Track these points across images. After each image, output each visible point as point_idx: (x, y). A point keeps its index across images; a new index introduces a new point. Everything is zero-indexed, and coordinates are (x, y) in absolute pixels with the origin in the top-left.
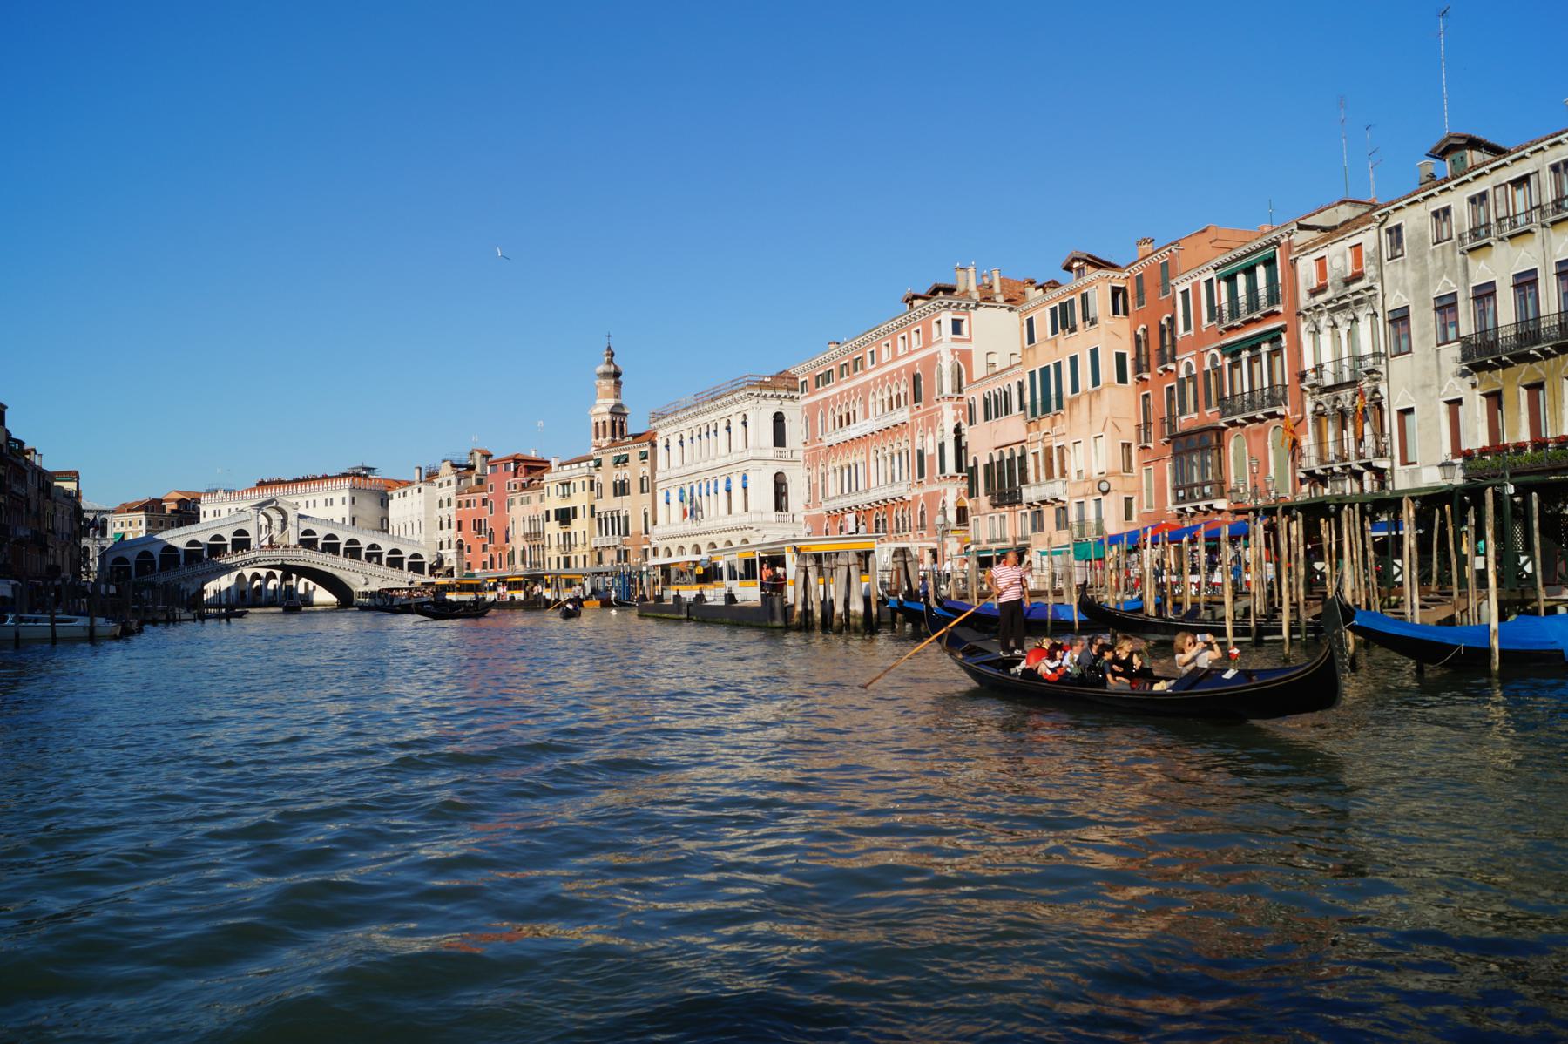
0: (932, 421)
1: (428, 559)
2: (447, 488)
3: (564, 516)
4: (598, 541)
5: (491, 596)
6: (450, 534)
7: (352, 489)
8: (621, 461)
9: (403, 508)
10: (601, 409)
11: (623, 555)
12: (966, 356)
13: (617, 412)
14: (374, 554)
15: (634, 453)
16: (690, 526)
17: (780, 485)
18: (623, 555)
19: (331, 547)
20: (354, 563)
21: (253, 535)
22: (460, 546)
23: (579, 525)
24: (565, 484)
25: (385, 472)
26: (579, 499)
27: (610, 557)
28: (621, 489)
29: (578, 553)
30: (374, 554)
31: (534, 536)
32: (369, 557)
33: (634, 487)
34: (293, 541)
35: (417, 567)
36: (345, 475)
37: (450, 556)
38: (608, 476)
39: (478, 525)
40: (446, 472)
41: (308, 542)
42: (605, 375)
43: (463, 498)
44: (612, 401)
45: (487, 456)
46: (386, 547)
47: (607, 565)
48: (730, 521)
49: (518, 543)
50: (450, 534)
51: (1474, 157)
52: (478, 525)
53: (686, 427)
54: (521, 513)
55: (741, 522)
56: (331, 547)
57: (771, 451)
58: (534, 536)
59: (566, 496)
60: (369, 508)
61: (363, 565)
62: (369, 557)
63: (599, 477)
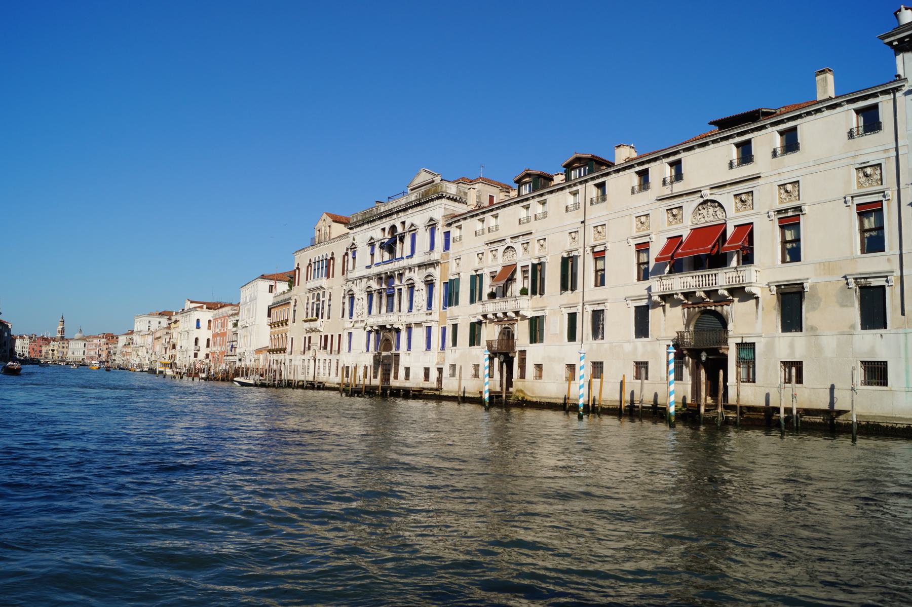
3: (53, 351)
26: (56, 348)
31: (47, 353)
38: (61, 345)
58: (47, 353)
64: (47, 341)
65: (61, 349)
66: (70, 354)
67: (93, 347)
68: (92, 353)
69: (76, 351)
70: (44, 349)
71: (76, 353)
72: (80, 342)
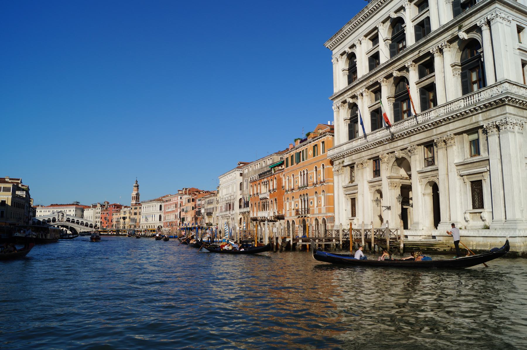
0: (177, 211)
1: (94, 225)
2: (99, 209)
3: (124, 218)
4: (130, 224)
5: (110, 233)
6: (99, 220)
8: (136, 208)
9: (87, 213)
10: (134, 194)
12: (182, 202)
13: (138, 194)
14: (82, 224)
15: (138, 207)
16: (146, 222)
17: (160, 217)
18: (135, 226)
19: (73, 222)
20: (78, 225)
22: (101, 222)
23: (127, 220)
24: (125, 212)
25: (82, 203)
26: (127, 215)
27: (133, 227)
28: (135, 214)
29: (126, 226)
30: (82, 224)
31: (118, 222)
32: (81, 224)
34: (65, 220)
35: (91, 226)
36: (73, 204)
37: (99, 224)
38: (133, 211)
39: (105, 218)
40: (99, 206)
41: (68, 220)
42: (135, 186)
43: (103, 212)
44: (136, 192)
45: (108, 203)
46: (85, 222)
47: (132, 228)
48: (152, 222)
49: (114, 223)
50: (99, 220)
51: (213, 195)
52: (105, 218)
54: (115, 217)
55: (154, 222)
56: (73, 222)
57: (159, 211)
58: (118, 222)
60: (79, 212)
61: (80, 226)
62: (81, 224)
63: (131, 211)
65: (133, 216)
66: (143, 221)
67: (172, 208)
68: (171, 218)
69: (150, 217)
70: (115, 217)
71: (150, 219)
72: (154, 203)
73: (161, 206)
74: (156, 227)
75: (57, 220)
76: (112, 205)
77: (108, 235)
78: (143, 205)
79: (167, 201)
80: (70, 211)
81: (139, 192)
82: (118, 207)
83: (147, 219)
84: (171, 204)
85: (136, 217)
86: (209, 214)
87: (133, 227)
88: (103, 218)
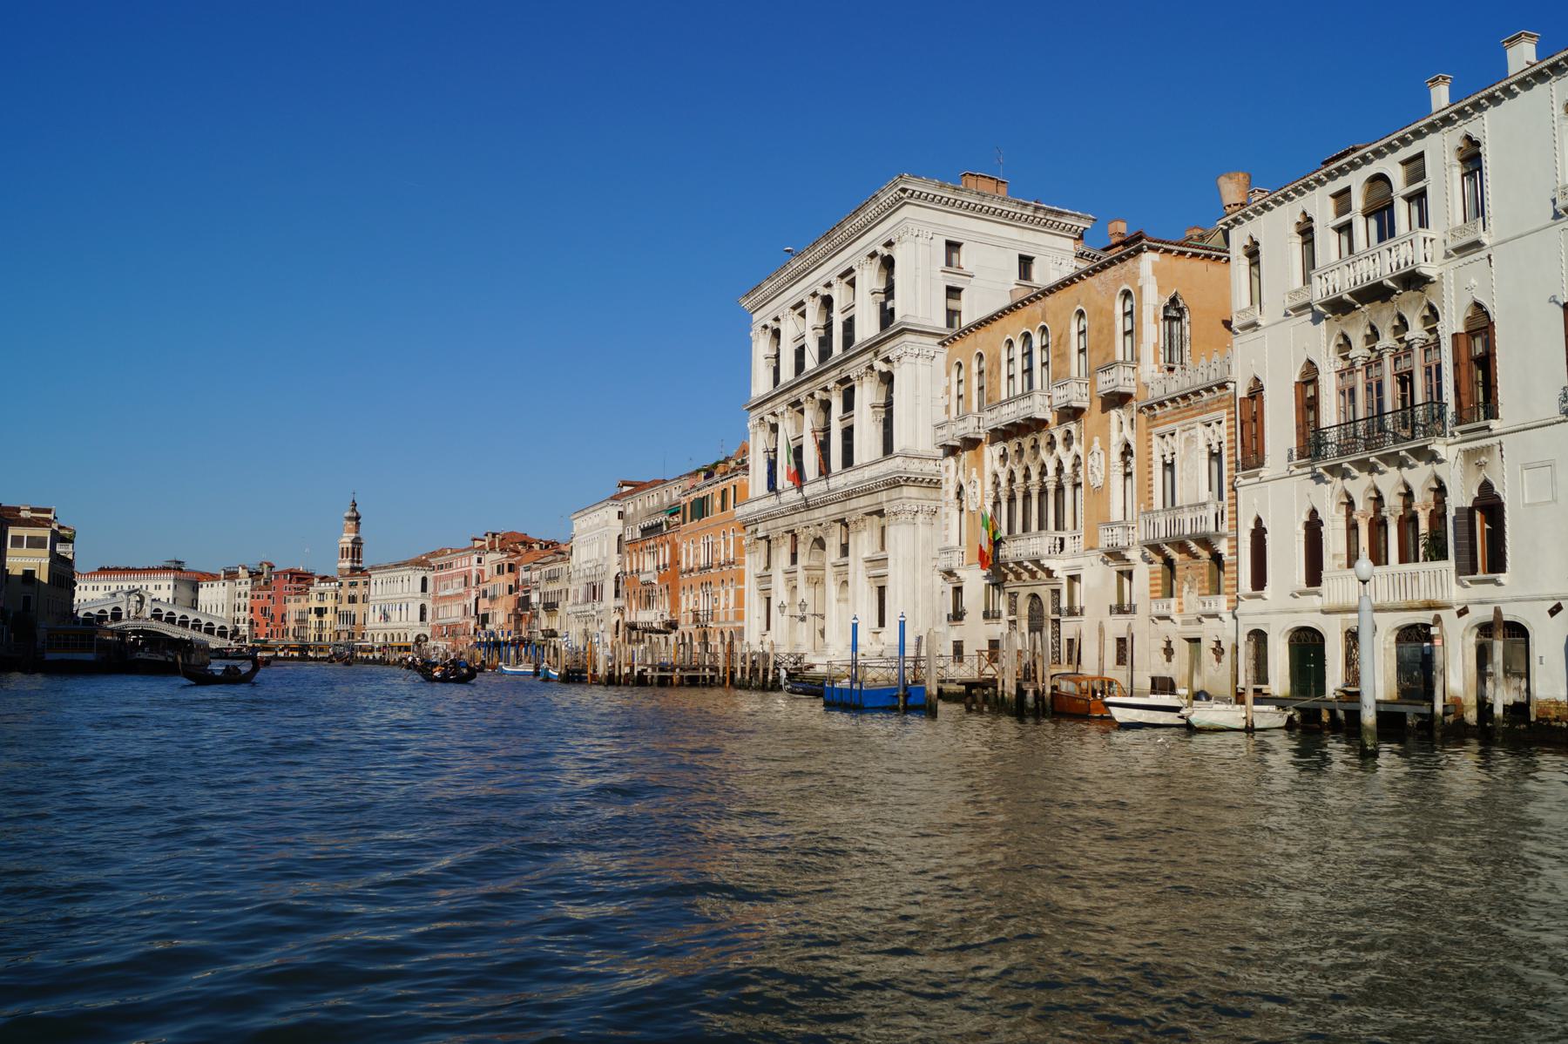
0: (469, 595)
1: (229, 629)
3: (320, 612)
4: (337, 627)
5: (281, 654)
6: (245, 615)
7: (175, 579)
10: (346, 540)
11: (351, 635)
12: (482, 572)
13: (357, 542)
15: (360, 581)
16: (383, 625)
18: (351, 635)
19: (171, 619)
21: (124, 611)
22: (251, 622)
23: (328, 618)
24: (322, 594)
25: (192, 564)
26: (329, 603)
27: (344, 636)
28: (352, 600)
29: (327, 633)
31: (302, 621)
32: (193, 627)
33: (360, 600)
34: (148, 615)
37: (244, 628)
38: (346, 592)
39: (264, 611)
41: (157, 615)
43: (257, 593)
45: (271, 567)
46: (204, 621)
47: (342, 640)
49: (291, 625)
50: (245, 615)
52: (264, 611)
53: (386, 576)
54: (293, 608)
55: (406, 625)
56: (171, 619)
58: (302, 621)
59: (322, 600)
60: (185, 592)
62: (193, 627)
64: (302, 579)
65: (345, 607)
66: (374, 620)
67: (456, 587)
68: (453, 613)
69: (395, 609)
70: (293, 608)
71: (395, 616)
72: (406, 573)
73: (424, 580)
74: (411, 639)
75: (124, 616)
76: (284, 573)
77: (276, 658)
78: (376, 577)
79: (441, 567)
80: (158, 587)
81: (361, 534)
82: (302, 579)
83: (386, 617)
84: (452, 576)
85: (354, 608)
86: (551, 607)
87: (344, 636)
88: (258, 611)
